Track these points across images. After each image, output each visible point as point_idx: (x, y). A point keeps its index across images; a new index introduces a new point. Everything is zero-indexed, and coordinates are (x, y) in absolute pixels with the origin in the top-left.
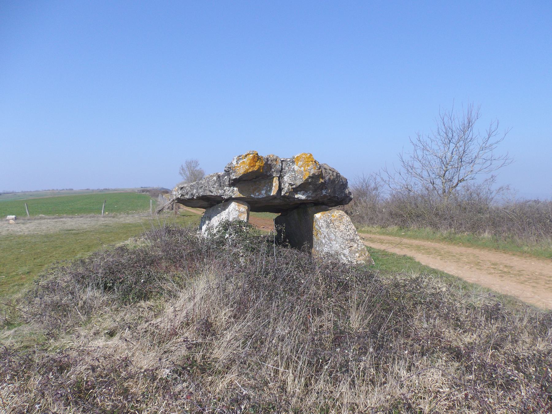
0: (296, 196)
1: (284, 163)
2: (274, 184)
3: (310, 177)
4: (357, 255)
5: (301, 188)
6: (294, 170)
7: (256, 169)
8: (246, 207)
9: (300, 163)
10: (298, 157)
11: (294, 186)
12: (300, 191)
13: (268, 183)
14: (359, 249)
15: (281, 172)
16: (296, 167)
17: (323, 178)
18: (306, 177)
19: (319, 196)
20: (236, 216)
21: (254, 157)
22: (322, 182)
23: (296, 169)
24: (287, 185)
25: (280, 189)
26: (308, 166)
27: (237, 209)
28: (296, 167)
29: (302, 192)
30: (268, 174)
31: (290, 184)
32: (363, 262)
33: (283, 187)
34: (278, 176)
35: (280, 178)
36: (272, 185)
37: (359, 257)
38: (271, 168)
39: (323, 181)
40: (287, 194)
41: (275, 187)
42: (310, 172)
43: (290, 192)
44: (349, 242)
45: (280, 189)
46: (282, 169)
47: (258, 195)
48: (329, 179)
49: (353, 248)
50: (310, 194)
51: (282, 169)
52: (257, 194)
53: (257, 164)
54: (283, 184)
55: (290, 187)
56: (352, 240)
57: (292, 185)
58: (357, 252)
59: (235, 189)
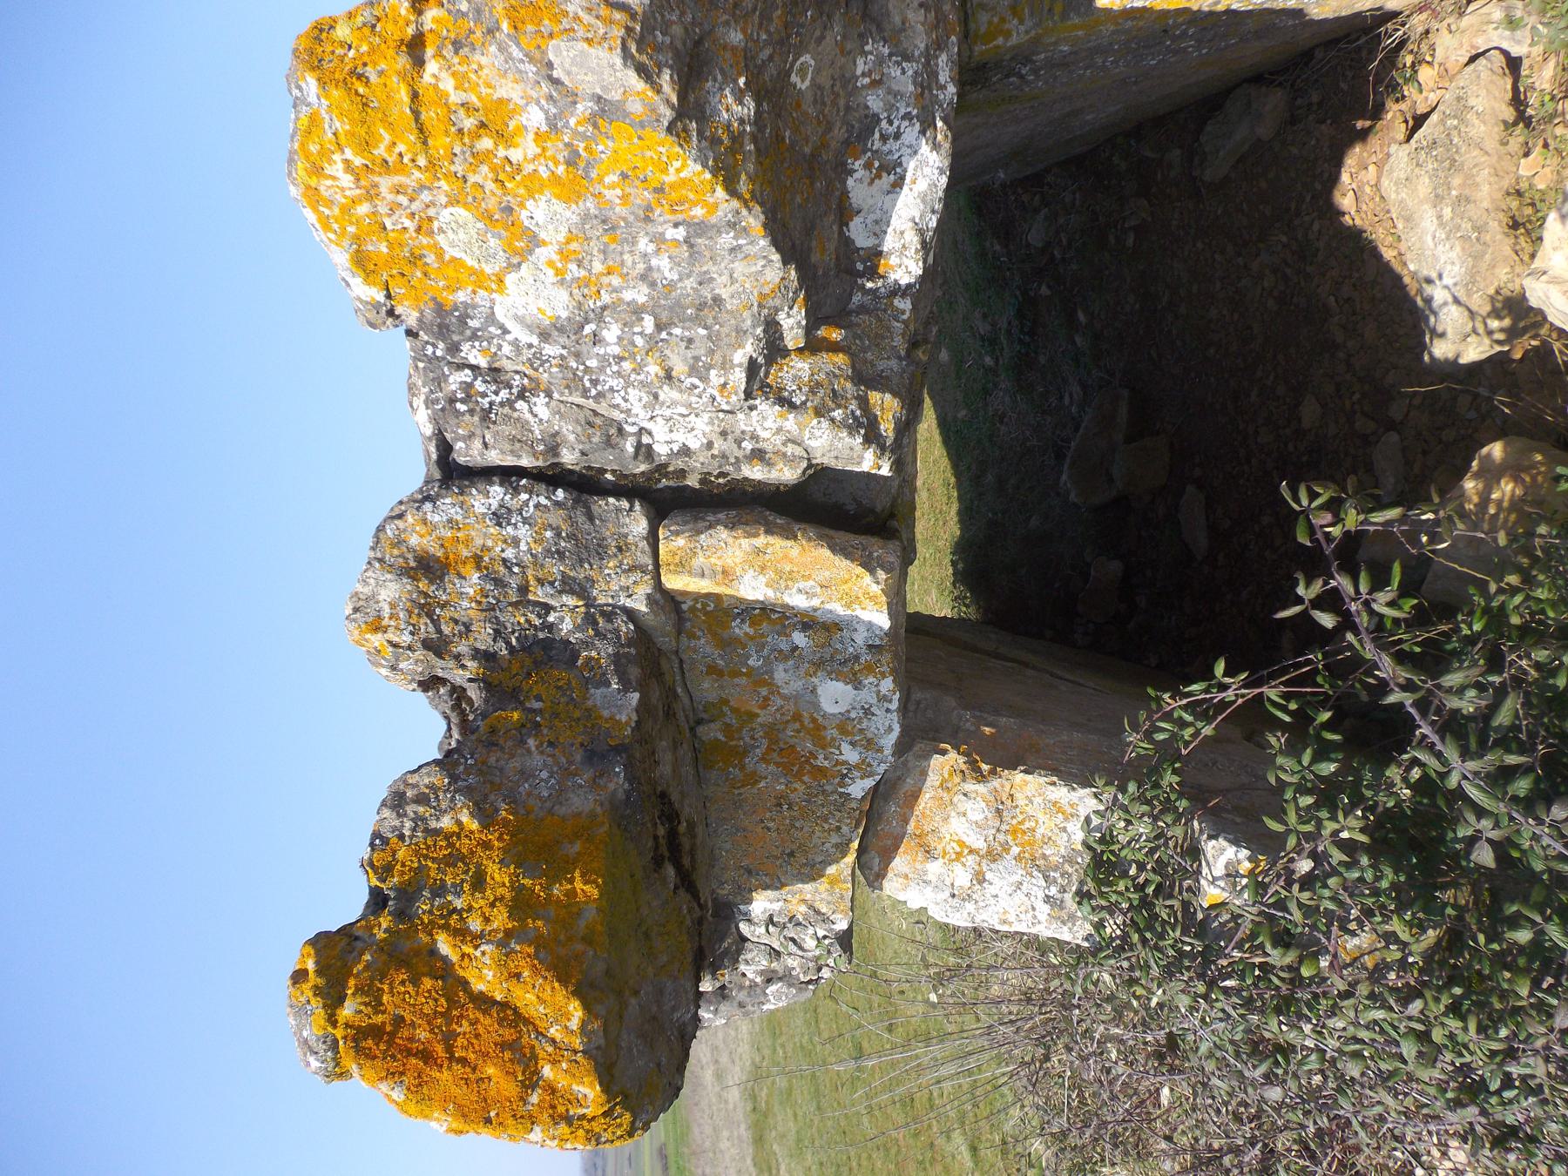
1: (468, 453)
2: (753, 588)
3: (690, 114)
5: (801, 188)
6: (574, 331)
7: (562, 1016)
8: (944, 764)
9: (459, 234)
10: (362, 262)
11: (792, 324)
12: (845, 212)
13: (728, 644)
15: (584, 485)
16: (525, 301)
18: (686, 168)
20: (1037, 887)
21: (379, 1046)
23: (560, 304)
24: (767, 421)
25: (823, 507)
26: (493, 122)
27: (962, 877)
28: (525, 301)
29: (858, 187)
30: (620, 704)
31: (757, 382)
33: (787, 474)
34: (638, 525)
35: (677, 499)
36: (763, 613)
38: (544, 651)
41: (785, 578)
42: (606, 111)
43: (866, 378)
45: (823, 507)
46: (552, 477)
47: (870, 744)
50: (903, 78)
51: (552, 477)
52: (851, 755)
53: (484, 976)
54: (755, 472)
55: (797, 370)
57: (774, 349)
59: (762, 904)
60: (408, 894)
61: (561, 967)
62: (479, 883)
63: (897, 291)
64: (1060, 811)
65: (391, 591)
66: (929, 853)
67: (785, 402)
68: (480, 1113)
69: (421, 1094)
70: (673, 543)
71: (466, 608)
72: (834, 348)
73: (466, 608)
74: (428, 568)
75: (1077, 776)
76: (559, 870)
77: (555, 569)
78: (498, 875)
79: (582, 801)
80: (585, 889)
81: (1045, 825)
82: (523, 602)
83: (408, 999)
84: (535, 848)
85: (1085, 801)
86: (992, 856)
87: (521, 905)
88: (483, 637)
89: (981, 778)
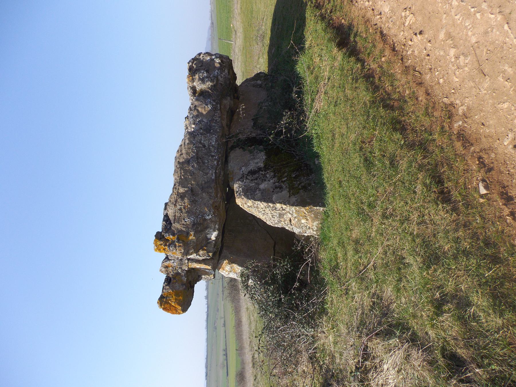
0: (214, 239)
2: (198, 267)
4: (303, 221)
8: (226, 262)
14: (295, 215)
17: (188, 234)
19: (213, 219)
22: (194, 236)
27: (227, 273)
32: (315, 223)
37: (307, 220)
38: (178, 274)
39: (192, 233)
40: (211, 254)
43: (208, 252)
44: (282, 220)
45: (204, 261)
48: (189, 212)
49: (293, 222)
56: (281, 216)
58: (299, 220)
60: (167, 297)
61: (179, 305)
62: (172, 297)
63: (213, 240)
64: (238, 269)
65: (163, 269)
66: (224, 270)
67: (200, 256)
68: (173, 313)
69: (168, 312)
70: (190, 264)
71: (170, 271)
72: (205, 250)
73: (170, 271)
74: (167, 267)
75: (239, 265)
76: (179, 297)
77: (179, 267)
78: (174, 297)
79: (181, 289)
80: (181, 298)
81: (236, 269)
82: (176, 270)
83: (166, 306)
84: (177, 295)
85: (240, 268)
86: (230, 271)
87: (176, 299)
88: (172, 273)
89: (229, 264)
